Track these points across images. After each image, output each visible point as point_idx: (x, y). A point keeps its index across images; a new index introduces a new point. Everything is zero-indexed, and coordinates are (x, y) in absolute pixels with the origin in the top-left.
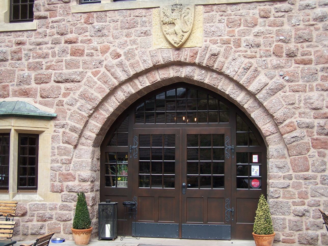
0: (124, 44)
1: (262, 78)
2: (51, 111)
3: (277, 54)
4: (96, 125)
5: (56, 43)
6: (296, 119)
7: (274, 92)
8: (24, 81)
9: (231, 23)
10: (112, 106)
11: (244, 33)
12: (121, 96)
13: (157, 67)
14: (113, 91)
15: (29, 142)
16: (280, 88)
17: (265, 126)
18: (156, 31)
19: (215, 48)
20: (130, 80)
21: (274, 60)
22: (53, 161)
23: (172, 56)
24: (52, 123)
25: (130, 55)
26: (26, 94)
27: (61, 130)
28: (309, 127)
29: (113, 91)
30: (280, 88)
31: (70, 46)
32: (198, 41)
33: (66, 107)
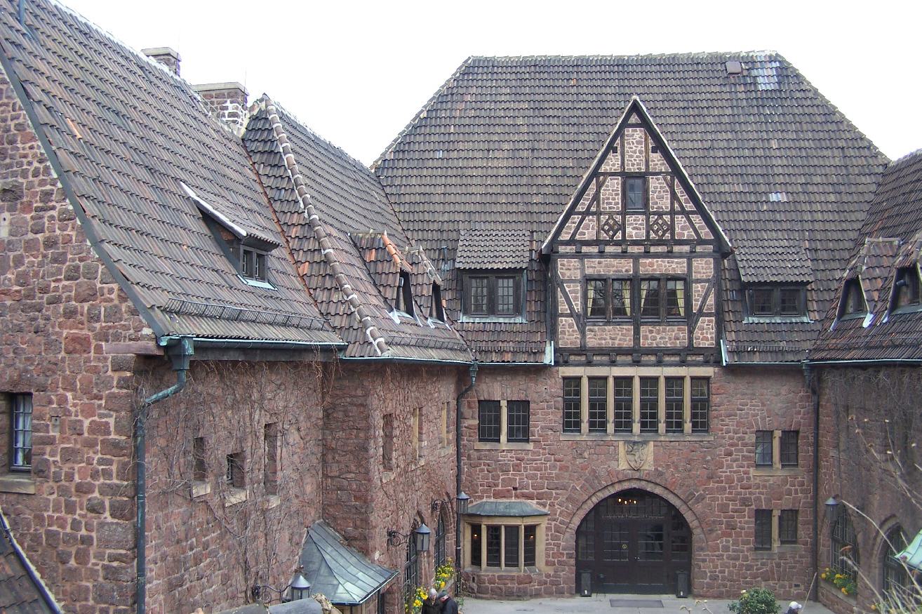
2: (546, 510)
5: (547, 460)
15: (531, 530)
22: (547, 544)
24: (546, 518)
27: (553, 523)
31: (558, 463)
33: (557, 506)
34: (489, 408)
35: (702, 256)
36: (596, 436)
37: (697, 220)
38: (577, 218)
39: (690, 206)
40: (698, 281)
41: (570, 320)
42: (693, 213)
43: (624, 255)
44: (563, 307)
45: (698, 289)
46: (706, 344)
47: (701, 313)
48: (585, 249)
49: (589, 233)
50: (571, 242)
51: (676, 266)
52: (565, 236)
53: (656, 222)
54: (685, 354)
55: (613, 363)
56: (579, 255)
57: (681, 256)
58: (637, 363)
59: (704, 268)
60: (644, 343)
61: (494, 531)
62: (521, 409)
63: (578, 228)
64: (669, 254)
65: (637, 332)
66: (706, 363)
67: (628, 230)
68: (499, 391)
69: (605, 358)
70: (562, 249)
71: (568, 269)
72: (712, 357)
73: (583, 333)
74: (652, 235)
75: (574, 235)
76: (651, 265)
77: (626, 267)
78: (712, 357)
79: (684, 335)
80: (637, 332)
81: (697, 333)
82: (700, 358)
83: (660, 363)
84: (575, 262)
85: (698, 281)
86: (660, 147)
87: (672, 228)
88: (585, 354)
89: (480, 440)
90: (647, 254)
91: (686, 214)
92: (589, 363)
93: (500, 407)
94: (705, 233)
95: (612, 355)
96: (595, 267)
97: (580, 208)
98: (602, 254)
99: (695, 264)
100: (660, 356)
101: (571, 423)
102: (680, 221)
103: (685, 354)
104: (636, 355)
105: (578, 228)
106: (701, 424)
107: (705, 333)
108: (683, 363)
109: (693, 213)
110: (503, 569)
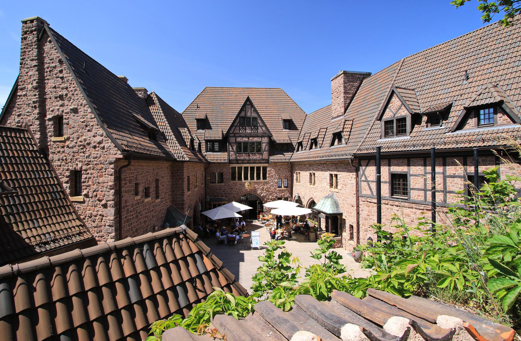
37: (264, 128)
40: (264, 143)
45: (264, 145)
50: (232, 133)
52: (231, 132)
59: (265, 140)
83: (255, 163)
84: (234, 138)
85: (264, 143)
88: (237, 161)
92: (238, 163)
97: (235, 125)
102: (260, 129)
104: (249, 162)
106: (265, 178)
107: (265, 155)
109: (262, 126)
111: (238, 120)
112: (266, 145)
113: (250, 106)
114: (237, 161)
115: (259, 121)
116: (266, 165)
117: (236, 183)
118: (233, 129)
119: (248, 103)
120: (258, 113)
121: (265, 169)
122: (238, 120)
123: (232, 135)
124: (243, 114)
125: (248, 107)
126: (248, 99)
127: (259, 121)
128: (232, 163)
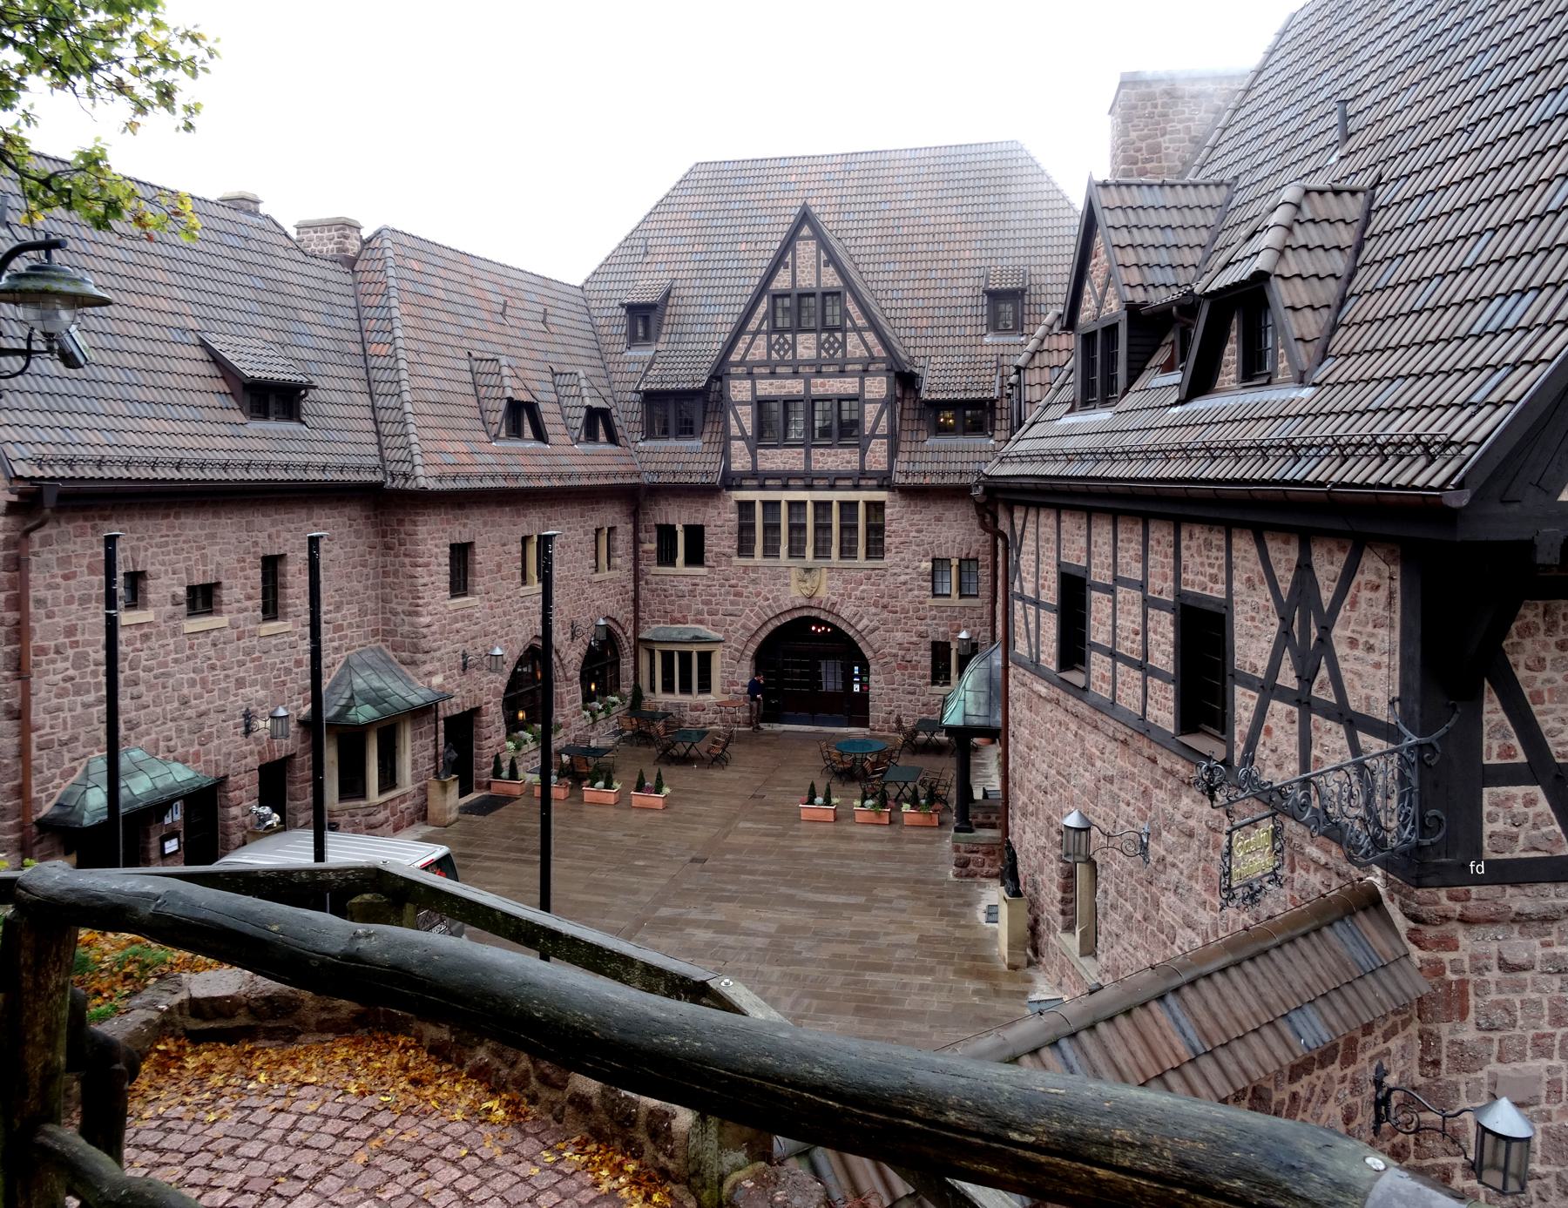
0: (771, 591)
1: (865, 622)
2: (720, 636)
3: (876, 605)
4: (753, 647)
5: (722, 586)
6: (887, 650)
7: (873, 631)
8: (700, 612)
9: (845, 581)
10: (763, 634)
11: (853, 589)
12: (770, 627)
13: (795, 609)
14: (765, 624)
15: (705, 658)
16: (877, 629)
17: (868, 654)
18: (794, 582)
19: (834, 598)
20: (777, 616)
21: (873, 610)
23: (804, 602)
25: (776, 599)
26: (701, 622)
28: (895, 656)
29: (765, 624)
30: (877, 629)
32: (823, 593)
34: (666, 534)
35: (877, 373)
36: (770, 561)
37: (870, 337)
38: (747, 338)
39: (861, 322)
41: (741, 444)
42: (865, 329)
43: (796, 374)
44: (735, 431)
45: (871, 411)
46: (880, 468)
47: (873, 436)
48: (756, 370)
49: (759, 351)
50: (741, 363)
51: (848, 386)
52: (735, 357)
53: (827, 340)
54: (858, 479)
55: (786, 487)
56: (750, 375)
57: (852, 374)
58: (809, 487)
59: (877, 387)
60: (816, 467)
61: (667, 657)
62: (696, 535)
63: (747, 350)
64: (842, 373)
65: (808, 457)
66: (880, 487)
67: (800, 349)
68: (679, 516)
69: (778, 482)
70: (733, 370)
71: (740, 390)
72: (884, 481)
73: (754, 456)
74: (824, 354)
75: (744, 356)
76: (823, 385)
77: (795, 387)
78: (884, 481)
79: (856, 458)
80: (808, 457)
81: (869, 456)
82: (874, 482)
83: (832, 487)
84: (747, 384)
86: (833, 260)
87: (843, 345)
88: (761, 479)
89: (659, 564)
90: (819, 373)
91: (858, 330)
92: (762, 487)
93: (676, 533)
94: (879, 351)
95: (785, 480)
96: (766, 388)
97: (753, 325)
98: (773, 374)
99: (867, 383)
100: (833, 481)
101: (745, 548)
102: (852, 339)
103: (858, 479)
104: (809, 480)
105: (747, 350)
106: (876, 548)
107: (877, 455)
108: (857, 487)
109: (865, 329)
110: (677, 697)
111: (763, 307)
112: (881, 413)
113: (812, 246)
114: (761, 479)
115: (852, 307)
116: (881, 496)
117: (756, 568)
118: (741, 346)
119: (806, 231)
120: (842, 272)
121: (876, 508)
122: (763, 307)
123: (740, 370)
124: (782, 281)
125: (806, 250)
126: (805, 217)
127: (852, 307)
128: (740, 487)
